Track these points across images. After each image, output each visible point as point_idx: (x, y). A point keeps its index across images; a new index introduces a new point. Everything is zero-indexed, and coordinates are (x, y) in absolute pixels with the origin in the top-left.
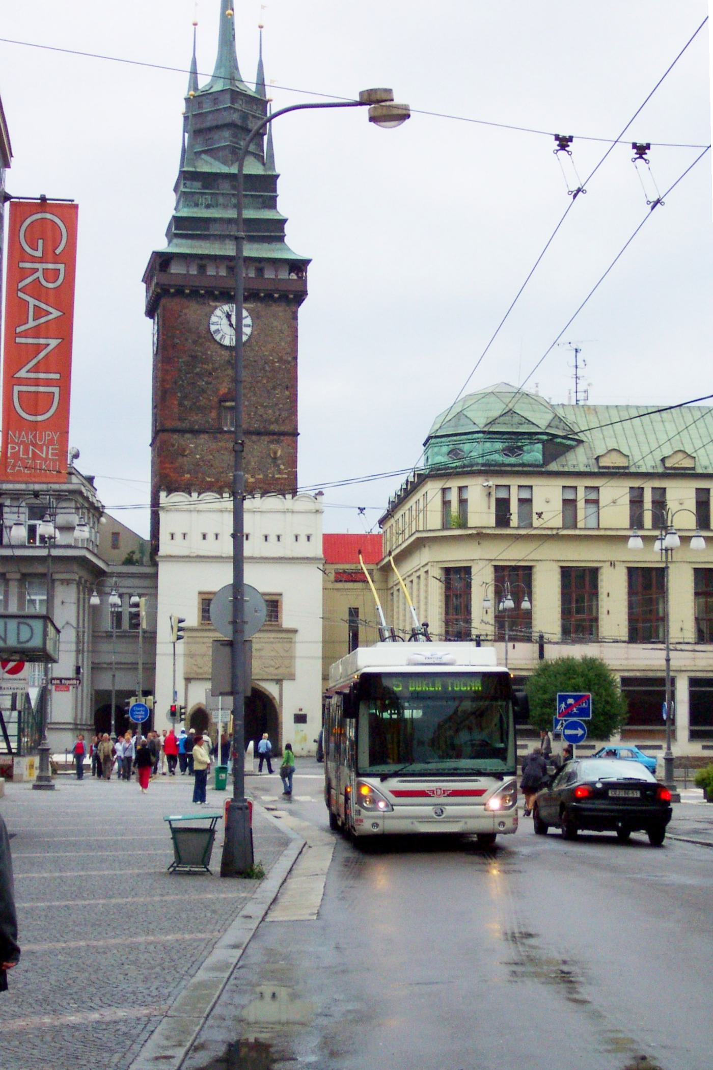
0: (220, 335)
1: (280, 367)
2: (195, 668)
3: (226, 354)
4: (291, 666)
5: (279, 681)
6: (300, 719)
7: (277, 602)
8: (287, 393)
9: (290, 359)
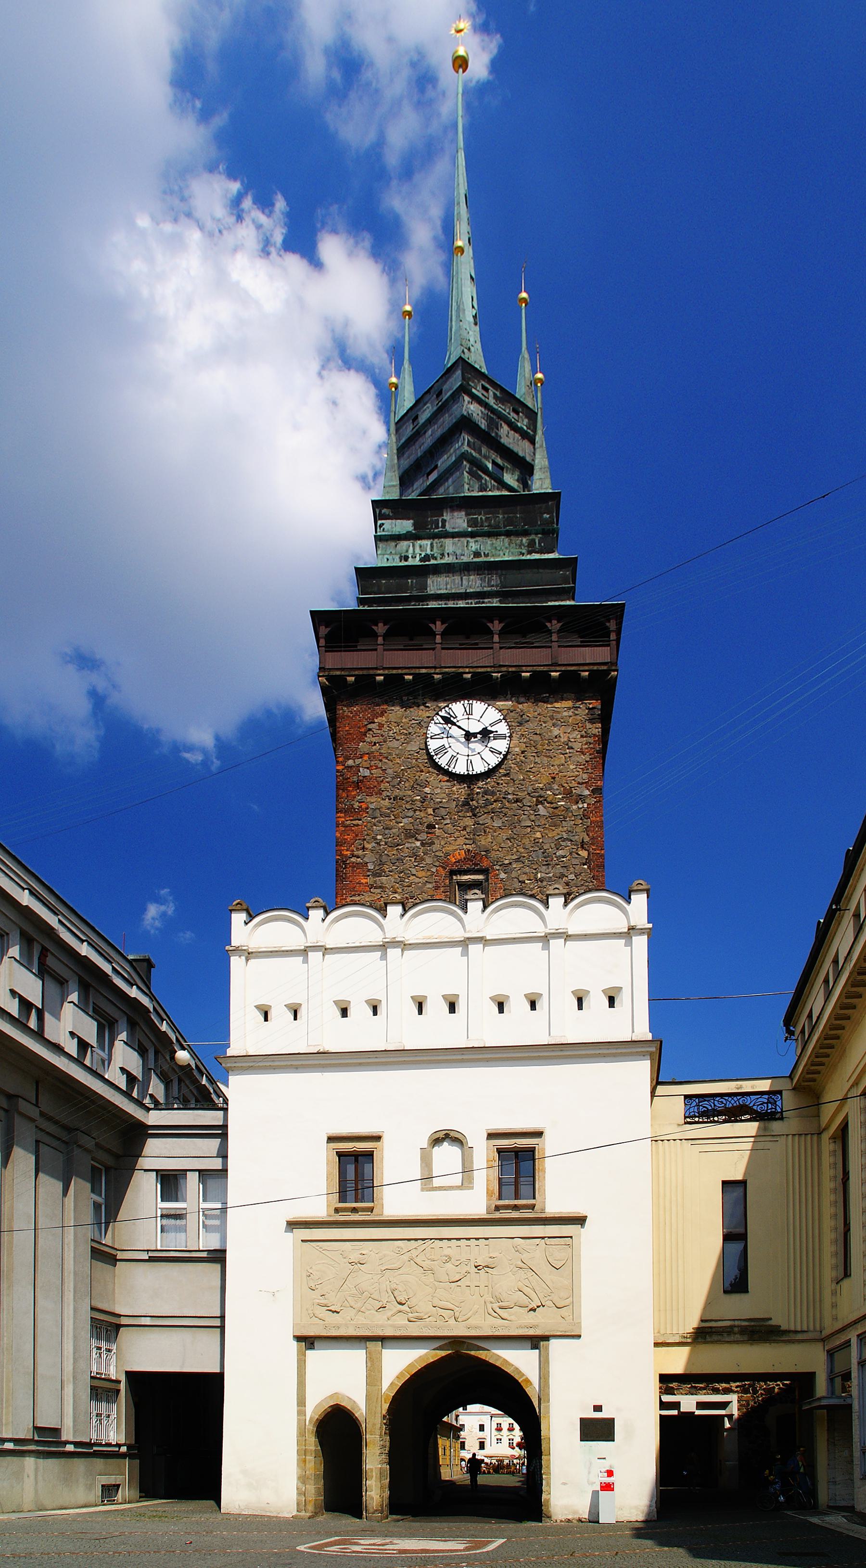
0: (447, 757)
1: (567, 809)
2: (322, 1312)
3: (460, 791)
4: (568, 1303)
5: (536, 1341)
6: (597, 1429)
7: (532, 1151)
8: (584, 854)
9: (587, 792)
